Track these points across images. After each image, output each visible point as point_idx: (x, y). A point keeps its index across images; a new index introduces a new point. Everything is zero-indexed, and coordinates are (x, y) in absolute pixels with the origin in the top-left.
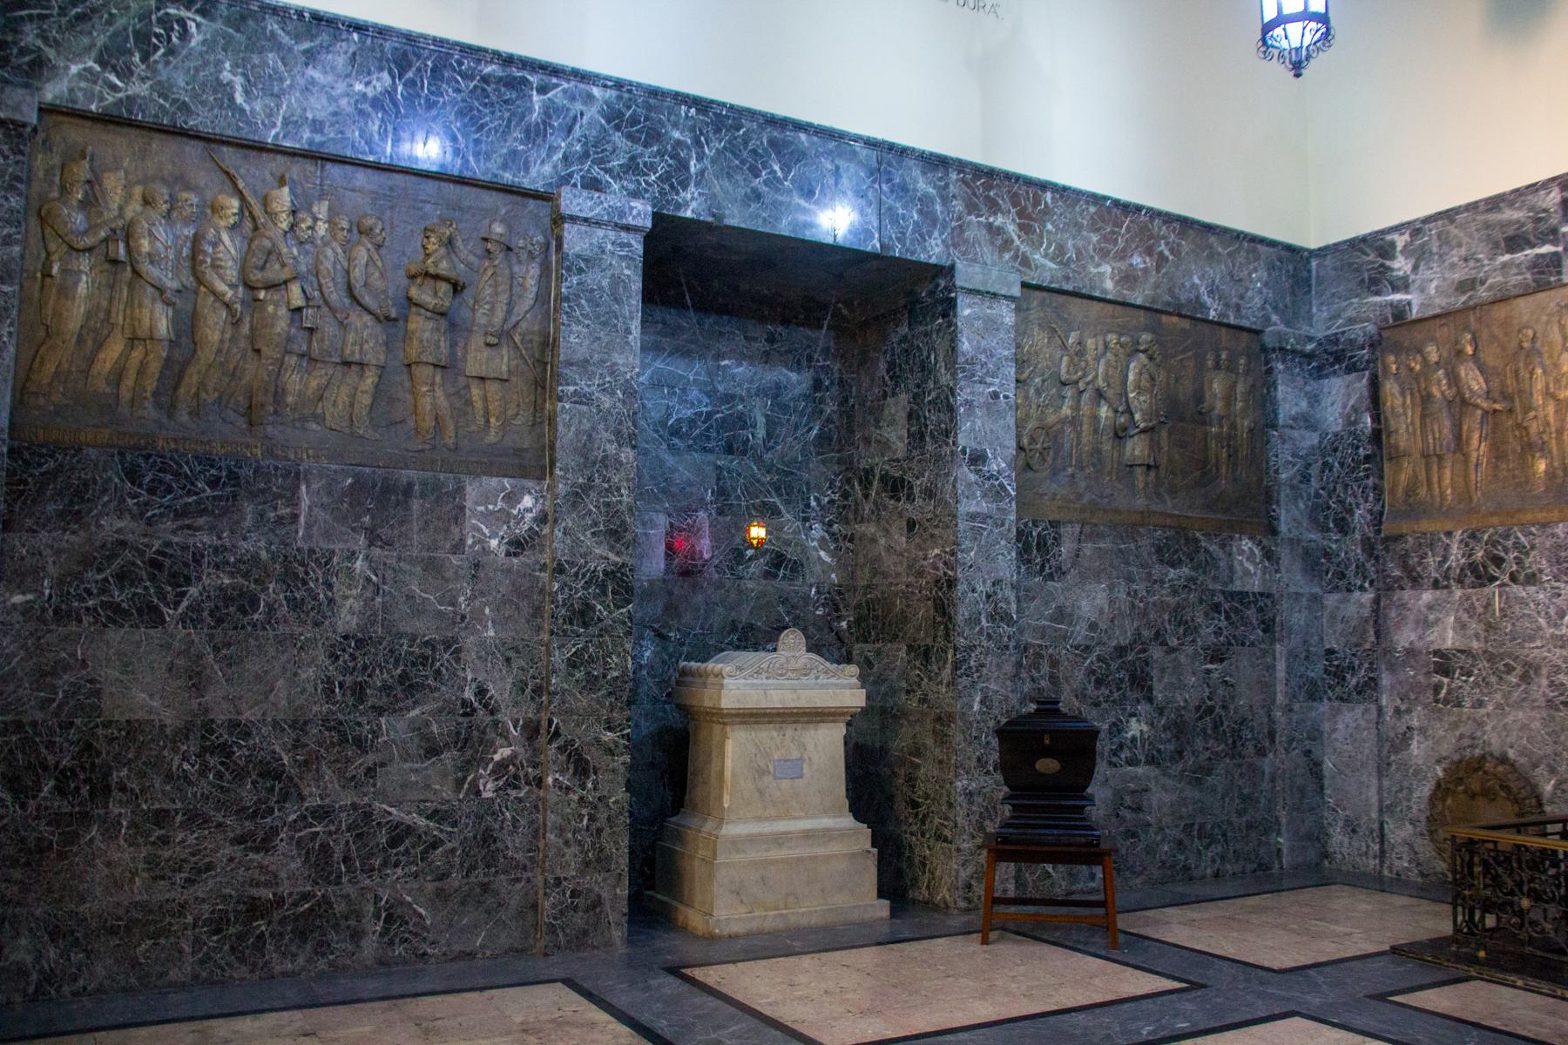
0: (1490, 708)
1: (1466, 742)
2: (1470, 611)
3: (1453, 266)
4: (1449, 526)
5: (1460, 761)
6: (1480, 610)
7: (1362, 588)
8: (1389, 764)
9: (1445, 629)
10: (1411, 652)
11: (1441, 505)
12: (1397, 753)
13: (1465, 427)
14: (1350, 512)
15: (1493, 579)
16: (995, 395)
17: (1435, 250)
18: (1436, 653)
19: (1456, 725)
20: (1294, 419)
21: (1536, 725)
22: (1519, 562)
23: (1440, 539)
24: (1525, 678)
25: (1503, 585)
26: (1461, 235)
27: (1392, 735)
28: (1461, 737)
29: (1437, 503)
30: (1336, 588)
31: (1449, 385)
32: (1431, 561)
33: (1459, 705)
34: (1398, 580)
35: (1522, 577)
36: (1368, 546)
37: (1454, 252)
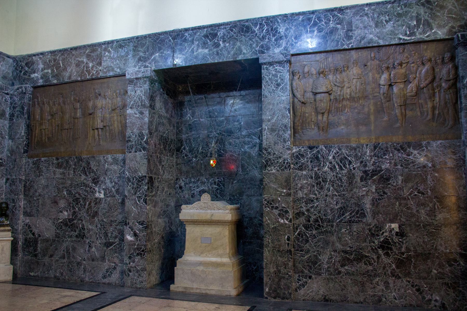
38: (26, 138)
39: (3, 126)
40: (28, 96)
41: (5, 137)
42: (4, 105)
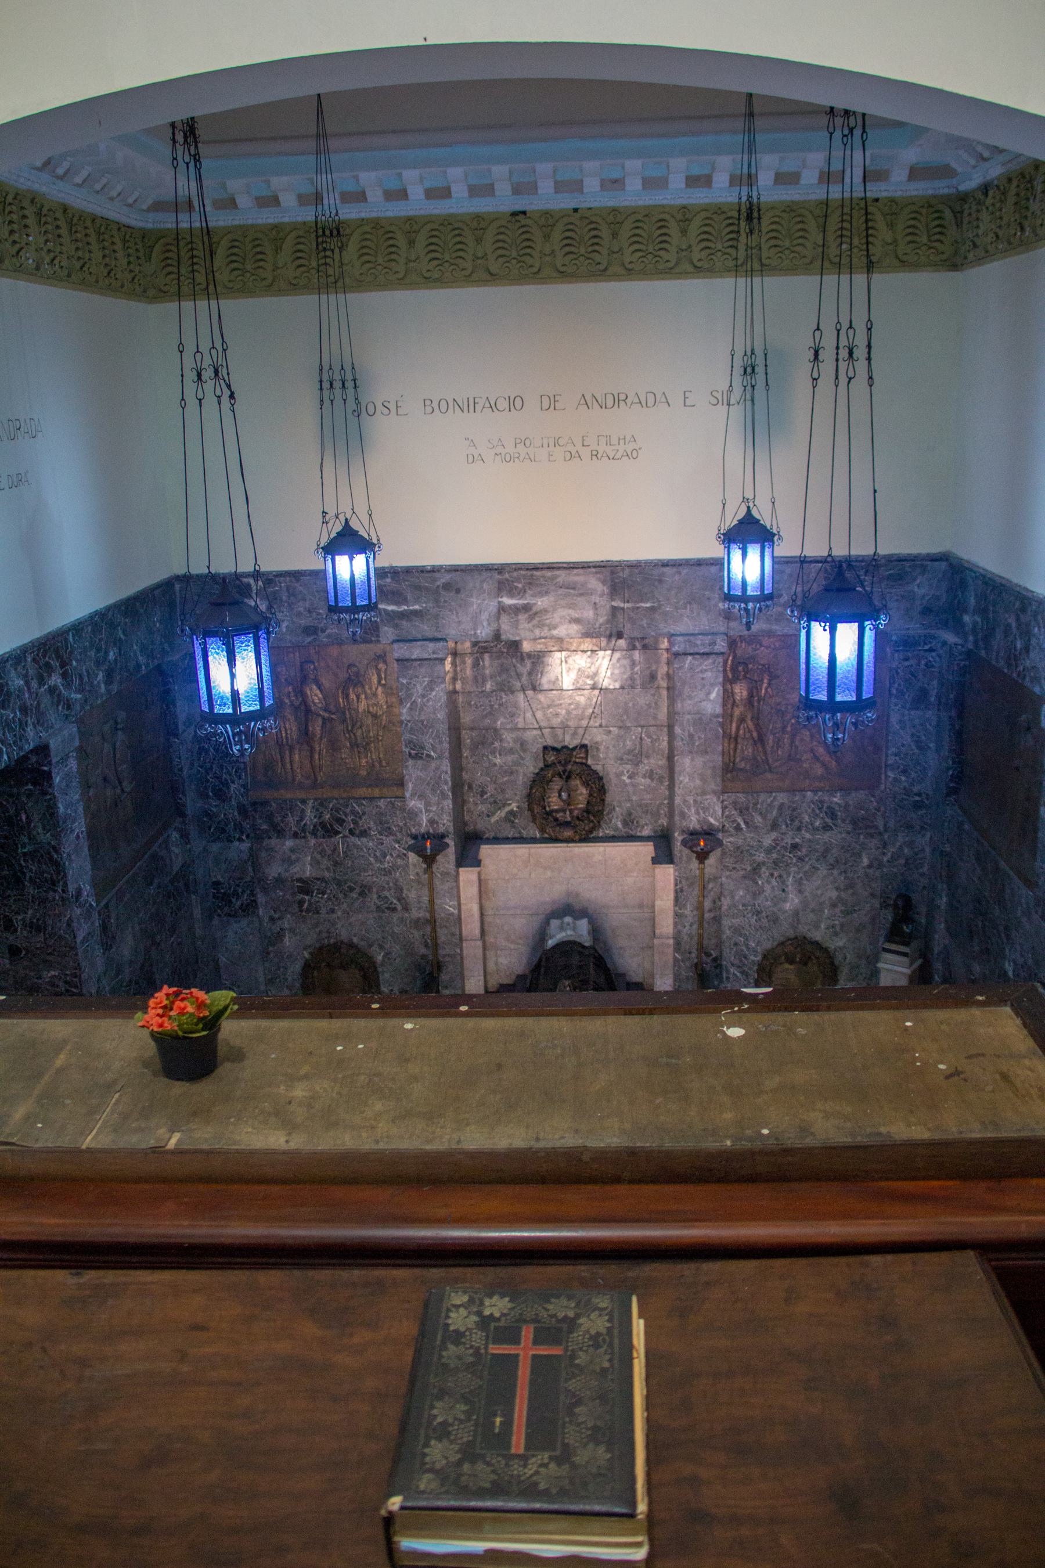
0: (339, 913)
1: (324, 935)
2: (322, 853)
3: (299, 614)
4: (301, 795)
5: (321, 948)
6: (330, 852)
7: (240, 840)
8: (268, 953)
9: (304, 865)
10: (279, 880)
11: (294, 780)
12: (274, 945)
13: (311, 729)
14: (226, 785)
15: (338, 833)
16: (78, 837)
17: (284, 598)
18: (299, 880)
19: (316, 925)
20: (184, 723)
21: (371, 922)
22: (355, 823)
23: (297, 805)
24: (362, 894)
25: (345, 836)
26: (305, 592)
27: (269, 934)
28: (320, 932)
29: (290, 778)
30: (218, 839)
31: (296, 696)
32: (291, 819)
33: (318, 913)
34: (266, 831)
35: (357, 832)
36: (242, 810)
37: (300, 604)
38: (954, 763)
39: (922, 725)
40: (958, 665)
41: (929, 748)
42: (924, 675)
